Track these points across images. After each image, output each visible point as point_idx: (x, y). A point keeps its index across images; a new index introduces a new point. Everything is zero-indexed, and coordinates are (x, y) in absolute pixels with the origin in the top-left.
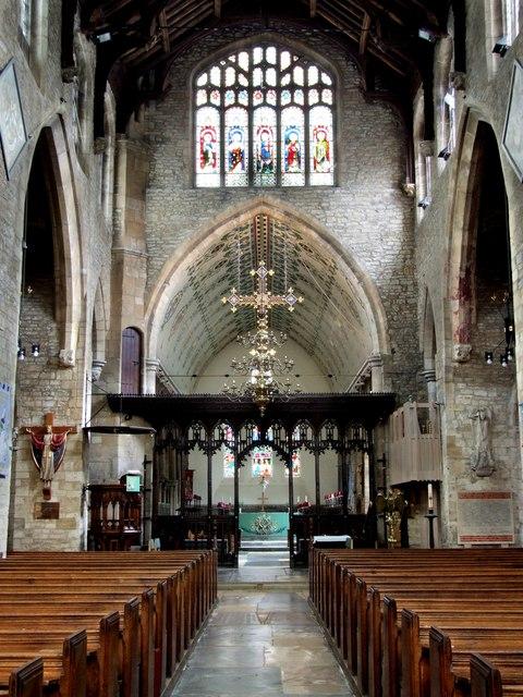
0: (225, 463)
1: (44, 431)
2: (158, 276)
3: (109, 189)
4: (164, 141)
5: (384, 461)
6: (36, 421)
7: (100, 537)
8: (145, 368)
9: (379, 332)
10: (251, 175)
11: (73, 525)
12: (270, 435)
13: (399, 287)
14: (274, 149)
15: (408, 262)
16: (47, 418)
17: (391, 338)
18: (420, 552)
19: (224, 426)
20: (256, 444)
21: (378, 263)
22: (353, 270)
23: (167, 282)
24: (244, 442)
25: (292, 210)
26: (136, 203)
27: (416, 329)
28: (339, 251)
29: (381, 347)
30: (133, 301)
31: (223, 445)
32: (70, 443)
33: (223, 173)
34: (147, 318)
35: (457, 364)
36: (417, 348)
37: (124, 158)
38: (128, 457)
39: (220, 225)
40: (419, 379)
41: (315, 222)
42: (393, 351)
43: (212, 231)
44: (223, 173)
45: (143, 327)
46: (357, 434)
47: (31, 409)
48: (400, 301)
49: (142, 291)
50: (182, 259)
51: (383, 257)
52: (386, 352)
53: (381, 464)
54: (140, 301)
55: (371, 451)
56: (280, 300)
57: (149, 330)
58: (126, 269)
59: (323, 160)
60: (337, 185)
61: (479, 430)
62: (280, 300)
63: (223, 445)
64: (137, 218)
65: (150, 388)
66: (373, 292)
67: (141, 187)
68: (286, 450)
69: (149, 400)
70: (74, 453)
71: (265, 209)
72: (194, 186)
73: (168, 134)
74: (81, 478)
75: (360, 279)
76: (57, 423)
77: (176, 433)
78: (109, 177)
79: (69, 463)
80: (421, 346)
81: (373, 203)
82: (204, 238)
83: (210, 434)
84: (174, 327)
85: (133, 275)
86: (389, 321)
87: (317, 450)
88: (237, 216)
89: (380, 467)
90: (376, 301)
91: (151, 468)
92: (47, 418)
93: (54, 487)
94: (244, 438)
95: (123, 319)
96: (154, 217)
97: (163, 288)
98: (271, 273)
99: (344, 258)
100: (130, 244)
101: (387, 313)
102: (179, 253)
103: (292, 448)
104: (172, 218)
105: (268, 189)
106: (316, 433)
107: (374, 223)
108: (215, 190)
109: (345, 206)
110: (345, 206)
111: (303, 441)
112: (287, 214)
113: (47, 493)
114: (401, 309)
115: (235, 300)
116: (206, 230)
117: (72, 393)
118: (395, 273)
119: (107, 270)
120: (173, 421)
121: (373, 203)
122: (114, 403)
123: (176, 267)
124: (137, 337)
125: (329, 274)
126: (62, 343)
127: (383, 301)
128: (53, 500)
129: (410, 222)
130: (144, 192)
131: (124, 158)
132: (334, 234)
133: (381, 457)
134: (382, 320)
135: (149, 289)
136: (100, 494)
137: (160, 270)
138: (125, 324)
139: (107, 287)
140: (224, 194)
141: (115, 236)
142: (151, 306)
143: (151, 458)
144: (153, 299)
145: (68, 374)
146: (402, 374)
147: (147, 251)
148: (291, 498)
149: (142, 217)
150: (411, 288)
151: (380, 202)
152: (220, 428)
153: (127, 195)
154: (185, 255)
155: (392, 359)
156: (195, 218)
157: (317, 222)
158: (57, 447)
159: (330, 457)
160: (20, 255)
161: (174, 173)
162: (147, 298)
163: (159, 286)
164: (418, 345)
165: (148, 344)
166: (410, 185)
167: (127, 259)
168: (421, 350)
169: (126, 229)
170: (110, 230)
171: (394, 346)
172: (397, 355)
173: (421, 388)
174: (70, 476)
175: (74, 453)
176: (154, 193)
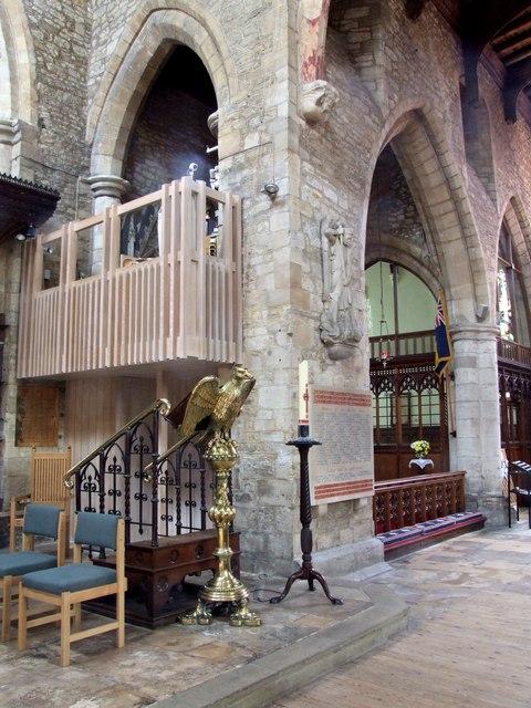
17: (39, 98)
29: (15, 110)
35: (303, 123)
36: (81, 133)
40: (80, 188)
52: (26, 115)
61: (338, 262)
80: (89, 132)
86: (40, 66)
114: (60, 57)
127: (31, 25)
134: (25, 60)
150: (79, 29)
164: (84, 129)
168: (88, 138)
171: (44, 115)
172: (47, 133)
173: (83, 206)
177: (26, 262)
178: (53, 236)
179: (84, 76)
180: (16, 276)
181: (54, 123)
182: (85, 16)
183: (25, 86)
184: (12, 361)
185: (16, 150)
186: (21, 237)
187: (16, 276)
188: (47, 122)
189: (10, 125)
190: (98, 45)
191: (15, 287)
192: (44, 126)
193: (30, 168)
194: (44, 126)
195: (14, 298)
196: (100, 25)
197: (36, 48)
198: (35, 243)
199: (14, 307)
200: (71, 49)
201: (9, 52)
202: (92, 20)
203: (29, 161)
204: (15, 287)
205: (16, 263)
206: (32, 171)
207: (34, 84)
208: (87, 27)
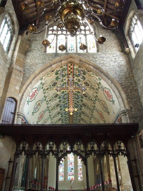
2: (27, 80)
4: (36, 40)
5: (135, 160)
8: (16, 116)
9: (123, 101)
12: (75, 148)
13: (129, 83)
14: (75, 46)
15: (131, 75)
17: (129, 103)
19: (51, 143)
20: (69, 152)
21: (118, 75)
22: (109, 79)
23: (31, 83)
24: (62, 151)
26: (22, 56)
29: (125, 107)
31: (51, 153)
34: (20, 95)
37: (19, 41)
39: (54, 64)
42: (131, 108)
43: (51, 66)
45: (18, 99)
46: (120, 147)
48: (131, 88)
49: (20, 84)
50: (38, 75)
51: (121, 73)
52: (127, 107)
53: (134, 162)
54: (18, 88)
55: (128, 155)
57: (21, 101)
58: (13, 75)
59: (93, 47)
60: (98, 51)
63: (51, 153)
64: (22, 60)
67: (25, 51)
68: (83, 155)
71: (71, 59)
73: (37, 39)
75: (112, 82)
81: (113, 56)
82: (48, 67)
83: (44, 147)
85: (16, 78)
89: (133, 164)
90: (120, 88)
91: (12, 164)
94: (62, 149)
95: (8, 93)
97: (29, 85)
99: (104, 74)
101: (126, 92)
102: (37, 72)
104: (35, 61)
106: (99, 146)
107: (115, 62)
108: (53, 54)
109: (103, 57)
111: (92, 150)
116: (48, 65)
118: (126, 78)
121: (113, 56)
123: (35, 77)
124: (14, 102)
125: (89, 120)
127: (123, 88)
131: (19, 41)
133: (133, 158)
134: (124, 96)
135: (23, 84)
137: (28, 78)
138: (8, 95)
141: (11, 64)
142: (22, 91)
143: (13, 160)
144: (24, 88)
146: (137, 117)
147: (24, 71)
151: (116, 56)
152: (49, 144)
153: (18, 52)
154: (39, 73)
155: (131, 111)
156: (44, 61)
157: (93, 62)
161: (38, 49)
162: (21, 88)
163: (27, 83)
165: (19, 106)
166: (127, 49)
167: (14, 71)
169: (16, 62)
171: (131, 105)
176: (31, 55)
177: (136, 142)
178: (140, 134)
179: (138, 93)
180: (135, 146)
181: (134, 106)
182: (134, 80)
183: (126, 101)
184: (140, 169)
185: (127, 116)
186: (133, 137)
187: (135, 146)
188: (132, 107)
189: (125, 111)
190: (139, 85)
191: (135, 149)
192: (132, 108)
193: (131, 119)
194: (132, 108)
195: (136, 152)
196: (138, 80)
197: (125, 92)
198: (137, 136)
199: (136, 154)
200: (133, 89)
201: (120, 96)
202: (136, 80)
203: (131, 118)
204: (135, 149)
205: (134, 143)
206: (132, 120)
207: (127, 100)
208: (135, 82)
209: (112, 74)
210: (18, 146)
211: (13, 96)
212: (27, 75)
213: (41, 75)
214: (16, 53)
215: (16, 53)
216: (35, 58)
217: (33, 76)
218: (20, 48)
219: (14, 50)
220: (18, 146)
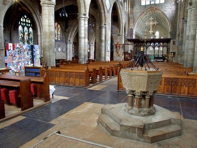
0: (151, 49)
1: (117, 45)
3: (127, 7)
6: (116, 43)
7: (126, 59)
9: (170, 28)
10: (150, 2)
11: (121, 57)
16: (118, 43)
17: (172, 29)
18: (103, 62)
20: (150, 46)
23: (136, 21)
25: (157, 8)
27: (177, 27)
28: (164, 14)
30: (131, 24)
32: (121, 46)
33: (146, 2)
38: (130, 47)
41: (160, 10)
44: (146, 2)
47: (116, 41)
54: (132, 24)
55: (167, 47)
56: (154, 23)
58: (130, 19)
60: (165, 3)
62: (154, 23)
65: (134, 37)
66: (170, 21)
67: (132, 6)
69: (134, 39)
70: (122, 47)
72: (141, 5)
74: (123, 51)
76: (119, 43)
77: (137, 44)
78: (127, 5)
79: (121, 49)
81: (171, 5)
84: (140, 27)
87: (159, 47)
88: (148, 9)
90: (170, 22)
92: (118, 43)
93: (119, 52)
96: (134, 11)
98: (153, 19)
100: (131, 16)
101: (172, 24)
102: (138, 16)
103: (155, 47)
105: (153, 4)
108: (144, 5)
110: (166, 6)
112: (156, 9)
113: (118, 53)
115: (147, 24)
117: (121, 39)
119: (127, 20)
120: (138, 42)
122: (129, 40)
126: (120, 32)
128: (119, 54)
129: (177, 9)
130: (133, 7)
132: (164, 11)
135: (134, 22)
136: (125, 53)
139: (127, 23)
140: (146, 6)
141: (128, 14)
145: (120, 37)
148: (163, 54)
149: (133, 11)
158: (119, 47)
159: (161, 49)
160: (110, 22)
166: (177, 2)
167: (130, 18)
170: (127, 14)
174: (121, 51)
175: (122, 47)
209: (168, 16)
210: (135, 44)
211: (131, 28)
212: (135, 18)
213: (140, 17)
214: (129, 9)
215: (129, 9)
216: (137, 10)
217: (137, 18)
218: (130, 6)
219: (128, 7)
220: (135, 44)
